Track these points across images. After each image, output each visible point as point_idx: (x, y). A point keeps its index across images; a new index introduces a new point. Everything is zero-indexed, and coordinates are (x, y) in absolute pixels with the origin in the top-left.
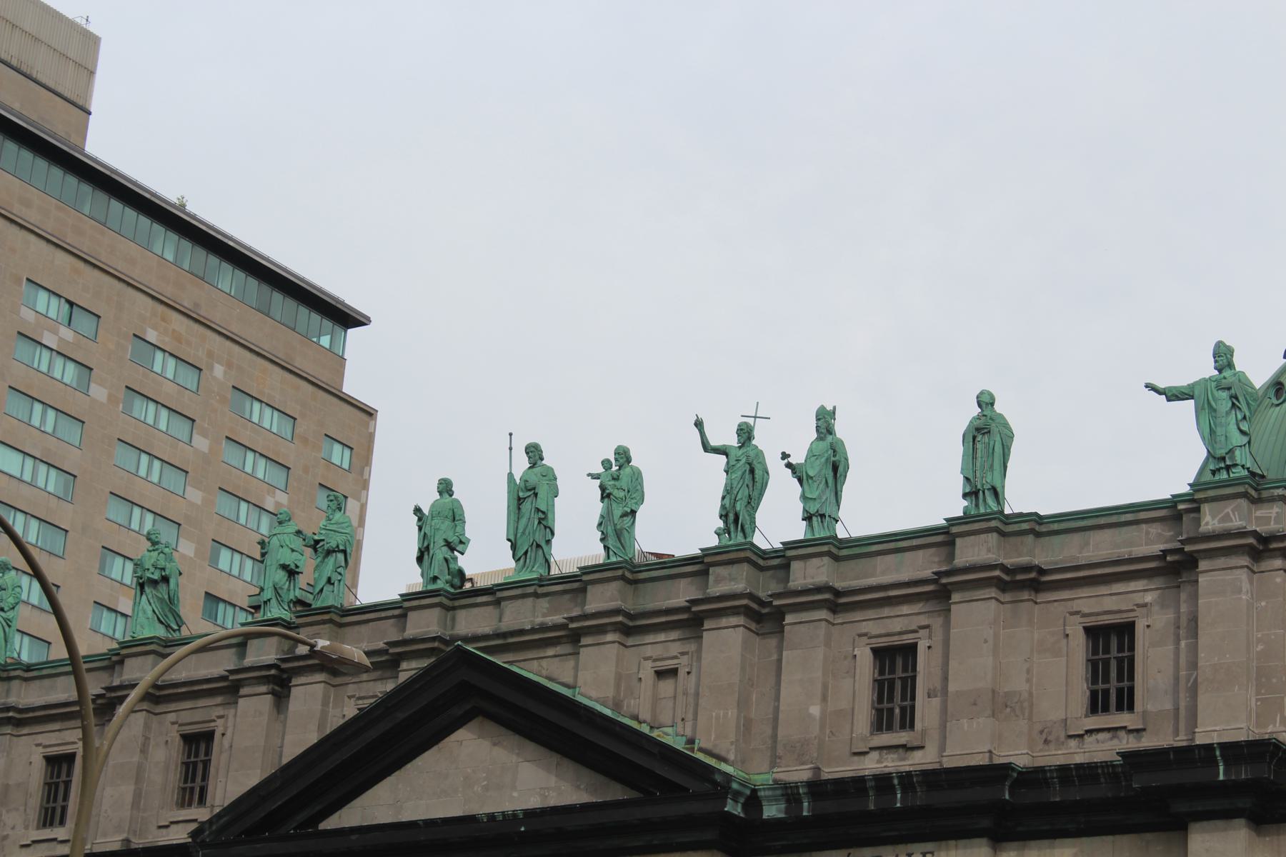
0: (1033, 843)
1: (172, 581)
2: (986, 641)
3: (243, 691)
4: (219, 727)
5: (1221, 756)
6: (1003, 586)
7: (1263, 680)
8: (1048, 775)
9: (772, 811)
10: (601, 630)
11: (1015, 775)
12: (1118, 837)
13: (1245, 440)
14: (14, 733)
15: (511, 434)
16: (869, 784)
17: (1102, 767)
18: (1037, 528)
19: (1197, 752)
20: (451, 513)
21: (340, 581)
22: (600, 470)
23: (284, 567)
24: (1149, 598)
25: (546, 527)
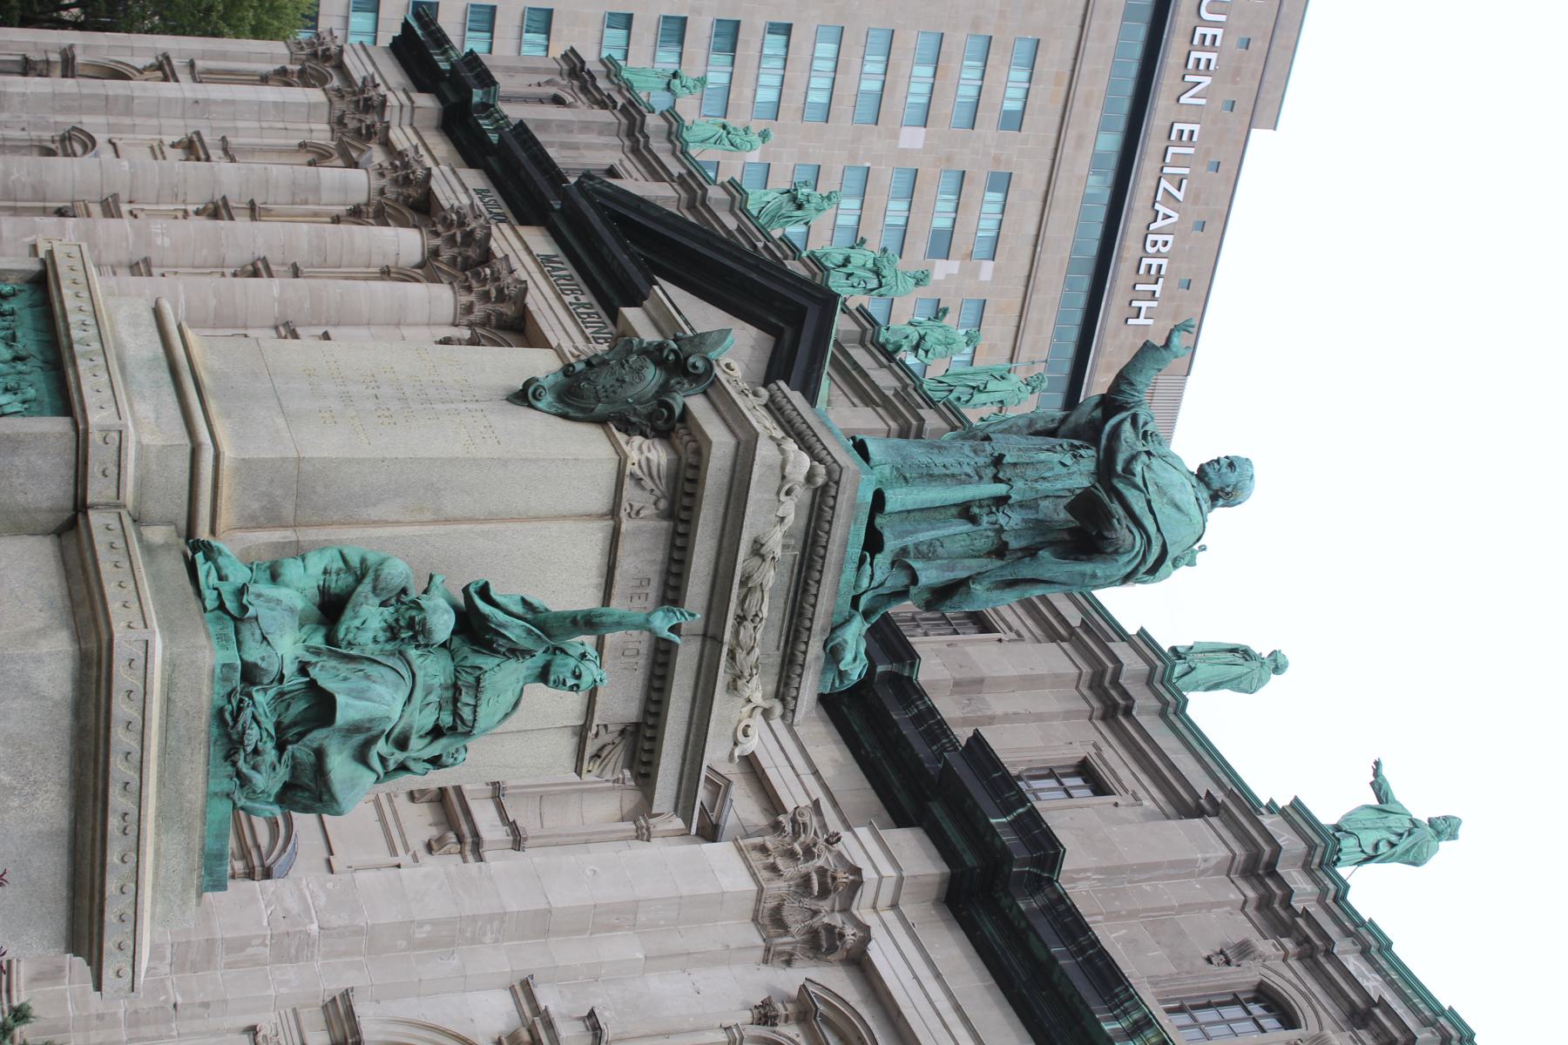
0: (833, 728)
1: (799, 213)
2: (1031, 669)
5: (1020, 815)
6: (1096, 685)
7: (1113, 895)
8: (919, 702)
10: (895, 414)
11: (906, 674)
12: (873, 792)
13: (1370, 851)
14: (626, 150)
17: (950, 741)
18: (1171, 710)
19: (1014, 793)
20: (951, 341)
21: (853, 286)
24: (1147, 803)
25: (972, 394)
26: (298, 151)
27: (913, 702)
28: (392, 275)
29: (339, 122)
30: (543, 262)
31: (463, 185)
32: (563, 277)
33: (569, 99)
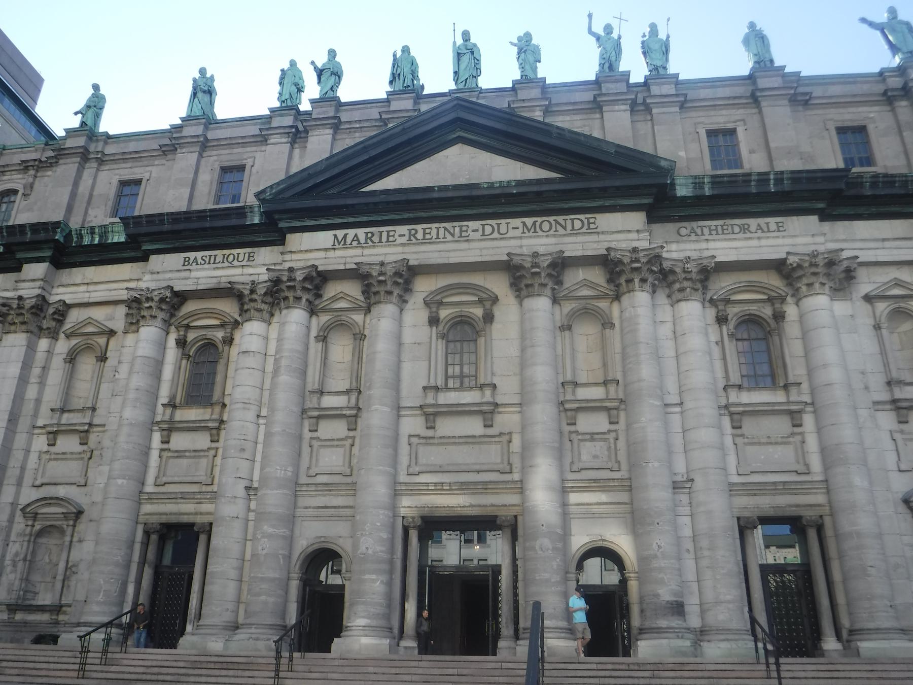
3: (272, 141)
4: (249, 163)
9: (683, 190)
15: (454, 24)
16: (754, 178)
22: (516, 41)
23: (296, 84)
26: (73, 364)
27: (862, 183)
28: (325, 334)
29: (40, 331)
30: (342, 243)
31: (178, 271)
32: (367, 238)
33: (19, 187)
